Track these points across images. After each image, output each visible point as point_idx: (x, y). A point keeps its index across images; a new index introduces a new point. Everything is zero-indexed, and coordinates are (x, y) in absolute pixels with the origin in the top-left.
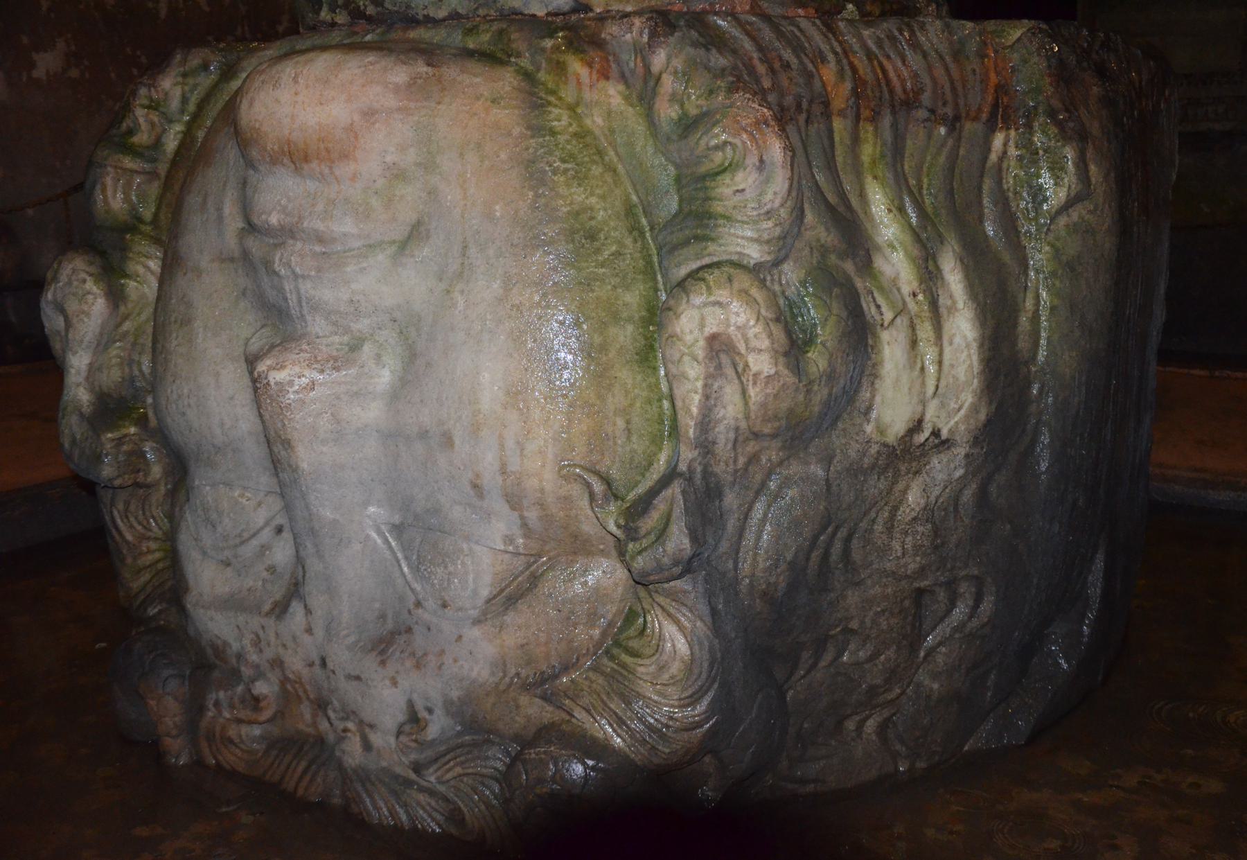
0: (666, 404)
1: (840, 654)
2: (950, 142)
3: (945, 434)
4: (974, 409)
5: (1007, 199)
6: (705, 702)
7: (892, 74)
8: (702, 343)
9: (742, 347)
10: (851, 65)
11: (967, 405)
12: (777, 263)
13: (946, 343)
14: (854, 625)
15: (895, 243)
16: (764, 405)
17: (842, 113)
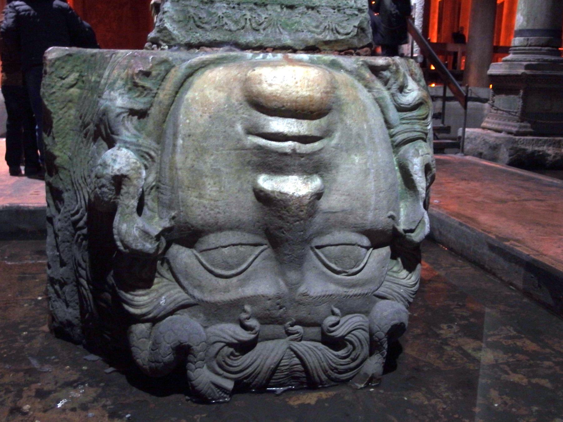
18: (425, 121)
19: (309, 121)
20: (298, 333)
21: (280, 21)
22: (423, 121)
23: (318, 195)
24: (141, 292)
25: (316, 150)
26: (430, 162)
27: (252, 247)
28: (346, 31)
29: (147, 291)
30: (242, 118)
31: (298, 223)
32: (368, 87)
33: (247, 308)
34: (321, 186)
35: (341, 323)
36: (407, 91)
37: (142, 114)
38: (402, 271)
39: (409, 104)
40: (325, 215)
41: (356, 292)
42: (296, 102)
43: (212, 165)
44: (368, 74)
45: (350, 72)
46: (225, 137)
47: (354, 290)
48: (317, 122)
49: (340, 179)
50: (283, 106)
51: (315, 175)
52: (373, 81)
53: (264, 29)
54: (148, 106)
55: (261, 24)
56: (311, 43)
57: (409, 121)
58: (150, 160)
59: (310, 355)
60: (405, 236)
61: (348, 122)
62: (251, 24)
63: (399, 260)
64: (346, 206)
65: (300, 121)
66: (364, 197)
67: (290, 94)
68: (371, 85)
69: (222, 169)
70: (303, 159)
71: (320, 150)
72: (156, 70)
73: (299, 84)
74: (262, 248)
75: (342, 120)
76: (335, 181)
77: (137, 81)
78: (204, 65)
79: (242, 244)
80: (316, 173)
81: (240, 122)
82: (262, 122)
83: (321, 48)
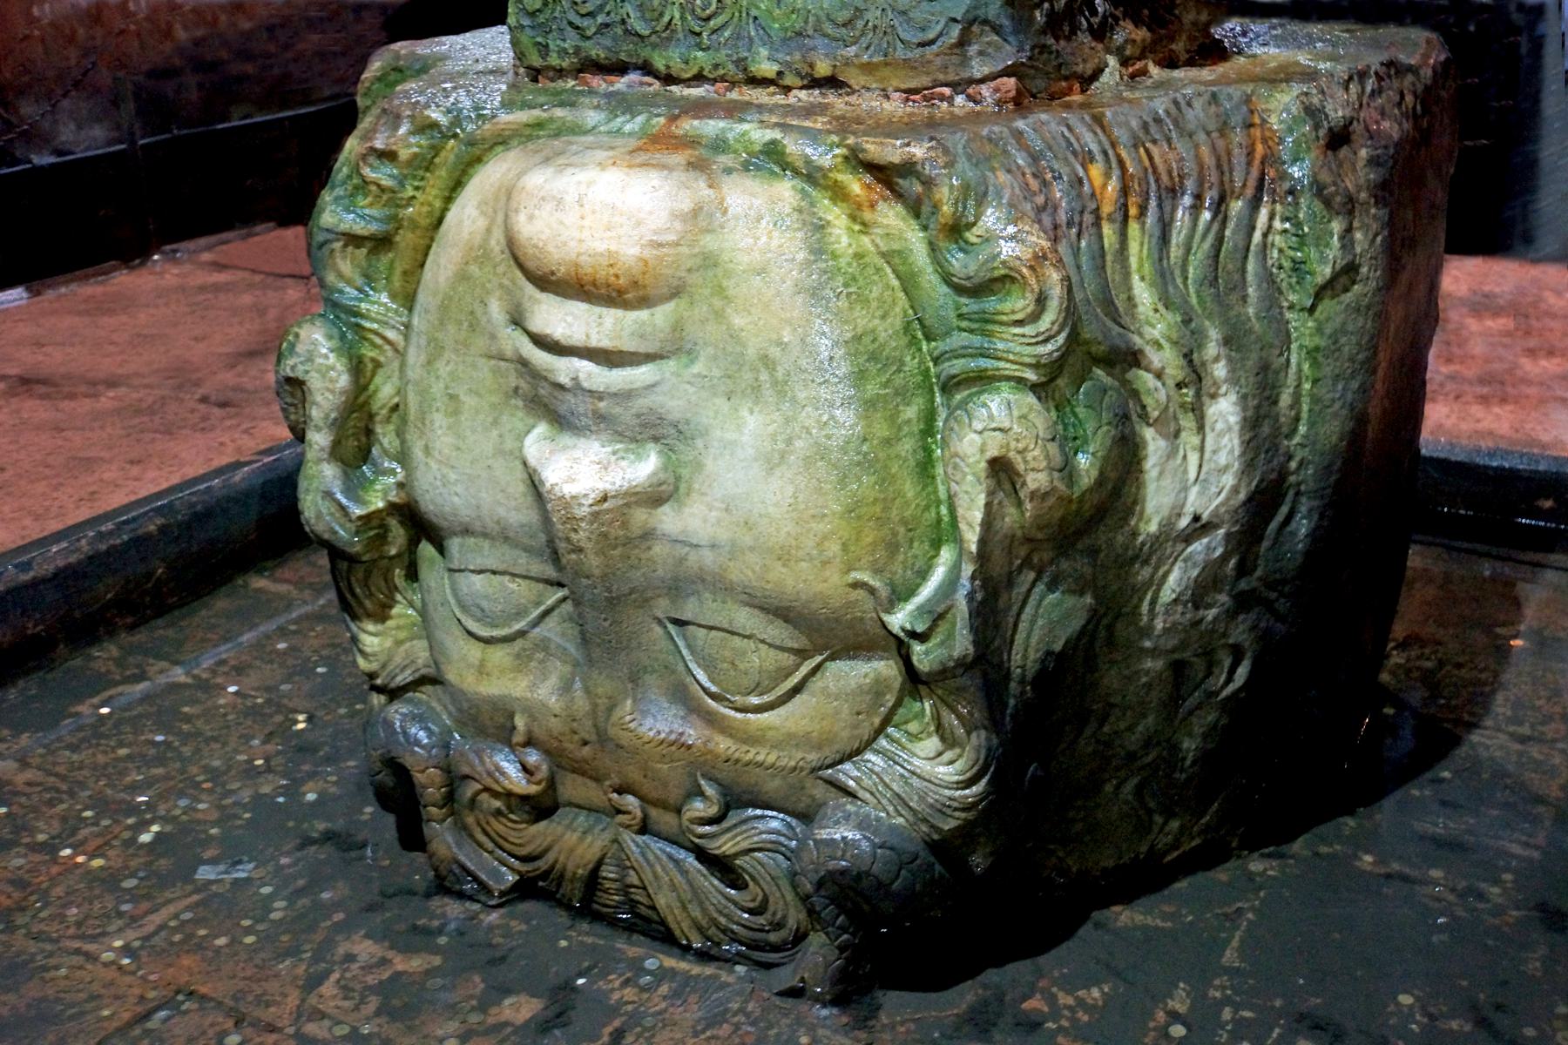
0: (944, 510)
1: (1101, 726)
2: (1216, 227)
3: (1205, 517)
4: (1235, 490)
5: (1271, 274)
6: (984, 781)
7: (1157, 160)
8: (983, 465)
9: (1021, 467)
10: (1118, 156)
11: (1228, 488)
12: (1052, 380)
13: (1207, 429)
14: (1116, 699)
15: (1162, 341)
16: (1037, 517)
17: (1110, 219)
18: (1028, 330)
19: (619, 313)
20: (629, 813)
21: (758, 8)
22: (1017, 330)
23: (655, 496)
24: (371, 627)
25: (638, 385)
26: (1012, 454)
27: (541, 586)
28: (921, 37)
29: (380, 627)
30: (501, 286)
31: (574, 556)
32: (858, 219)
33: (520, 722)
34: (654, 474)
35: (725, 825)
36: (973, 239)
37: (381, 243)
38: (929, 735)
39: (969, 278)
40: (678, 546)
41: (760, 758)
42: (577, 265)
43: (447, 388)
44: (856, 185)
45: (812, 176)
46: (471, 325)
47: (753, 751)
48: (643, 314)
49: (710, 465)
50: (553, 273)
51: (651, 445)
52: (872, 206)
53: (714, 32)
54: (391, 227)
55: (708, 19)
56: (823, 69)
57: (975, 326)
58: (387, 347)
59: (656, 877)
60: (909, 647)
61: (738, 321)
62: (683, 18)
63: (927, 705)
64: (723, 535)
65: (598, 310)
66: (766, 520)
67: (565, 244)
68: (867, 215)
69: (462, 397)
70: (602, 405)
71: (651, 387)
72: (409, 146)
73: (586, 223)
74: (560, 594)
75: (719, 315)
76: (698, 466)
77: (366, 171)
78: (502, 141)
79: (514, 575)
80: (656, 439)
81: (498, 294)
82: (527, 304)
83: (852, 82)
